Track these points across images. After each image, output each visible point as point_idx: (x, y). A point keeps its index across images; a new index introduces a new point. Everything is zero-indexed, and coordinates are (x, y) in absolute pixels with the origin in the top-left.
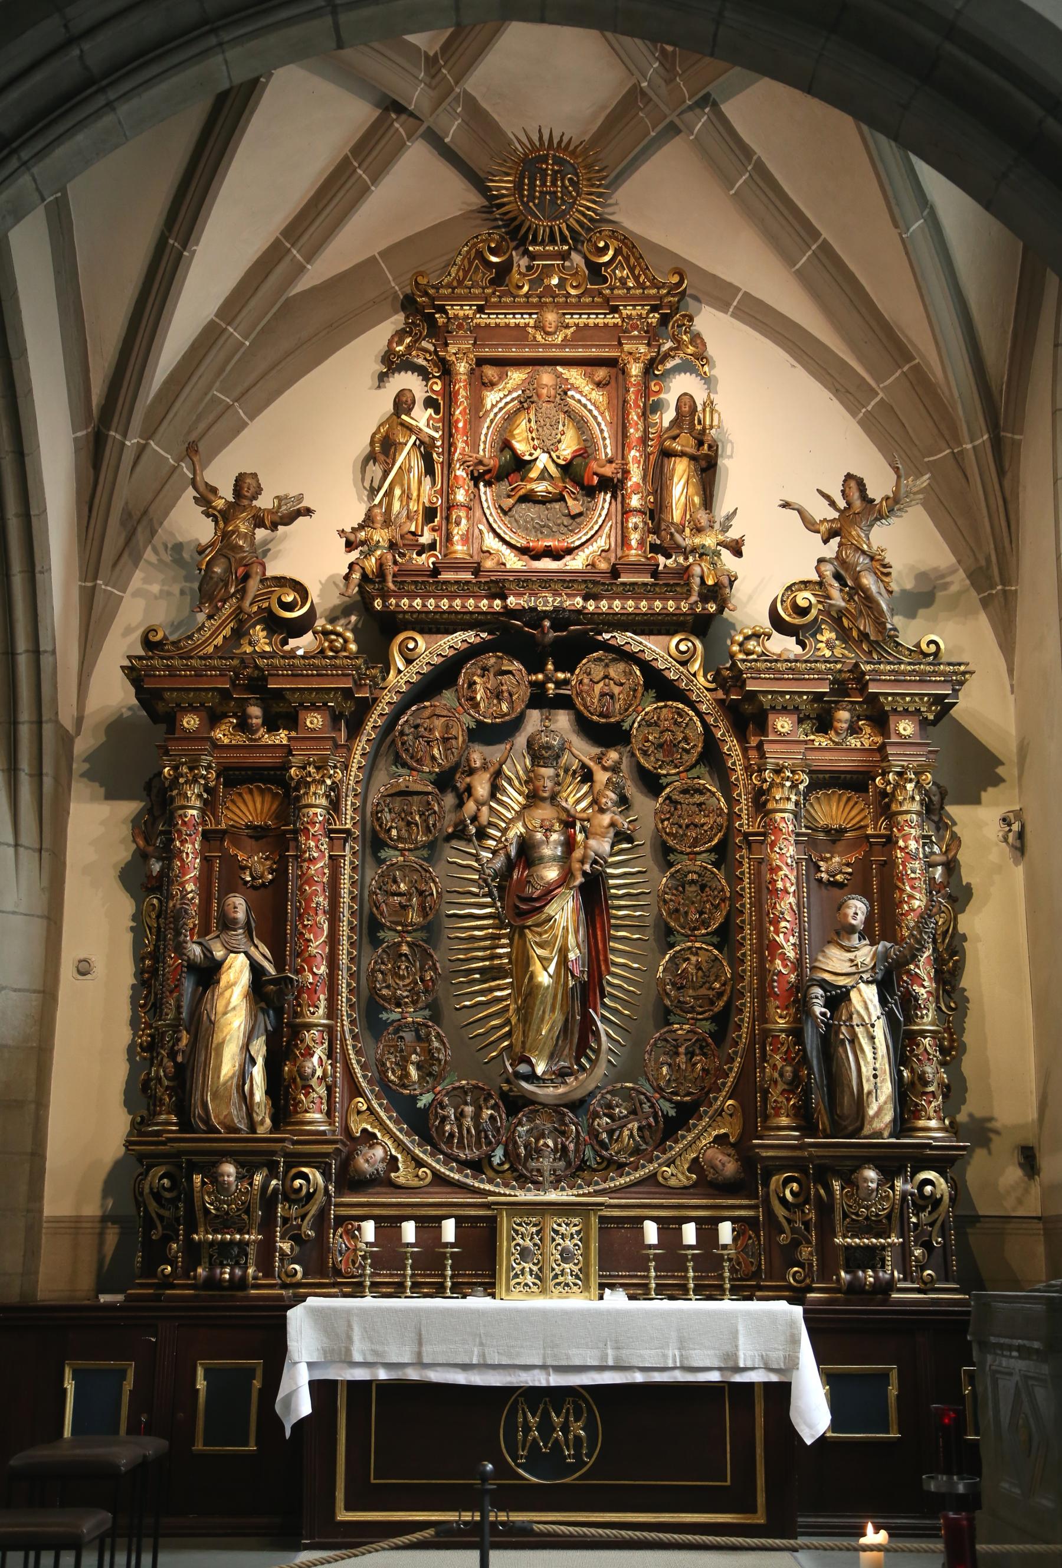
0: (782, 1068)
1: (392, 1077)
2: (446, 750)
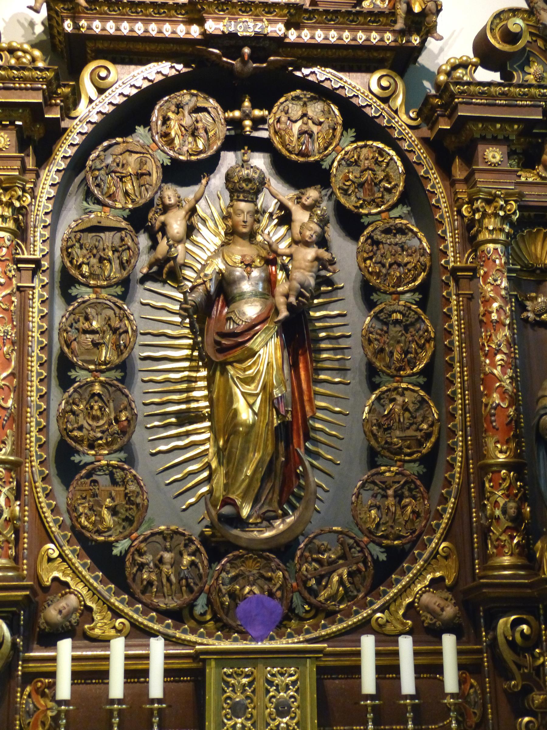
0: (505, 504)
1: (86, 523)
2: (140, 186)
